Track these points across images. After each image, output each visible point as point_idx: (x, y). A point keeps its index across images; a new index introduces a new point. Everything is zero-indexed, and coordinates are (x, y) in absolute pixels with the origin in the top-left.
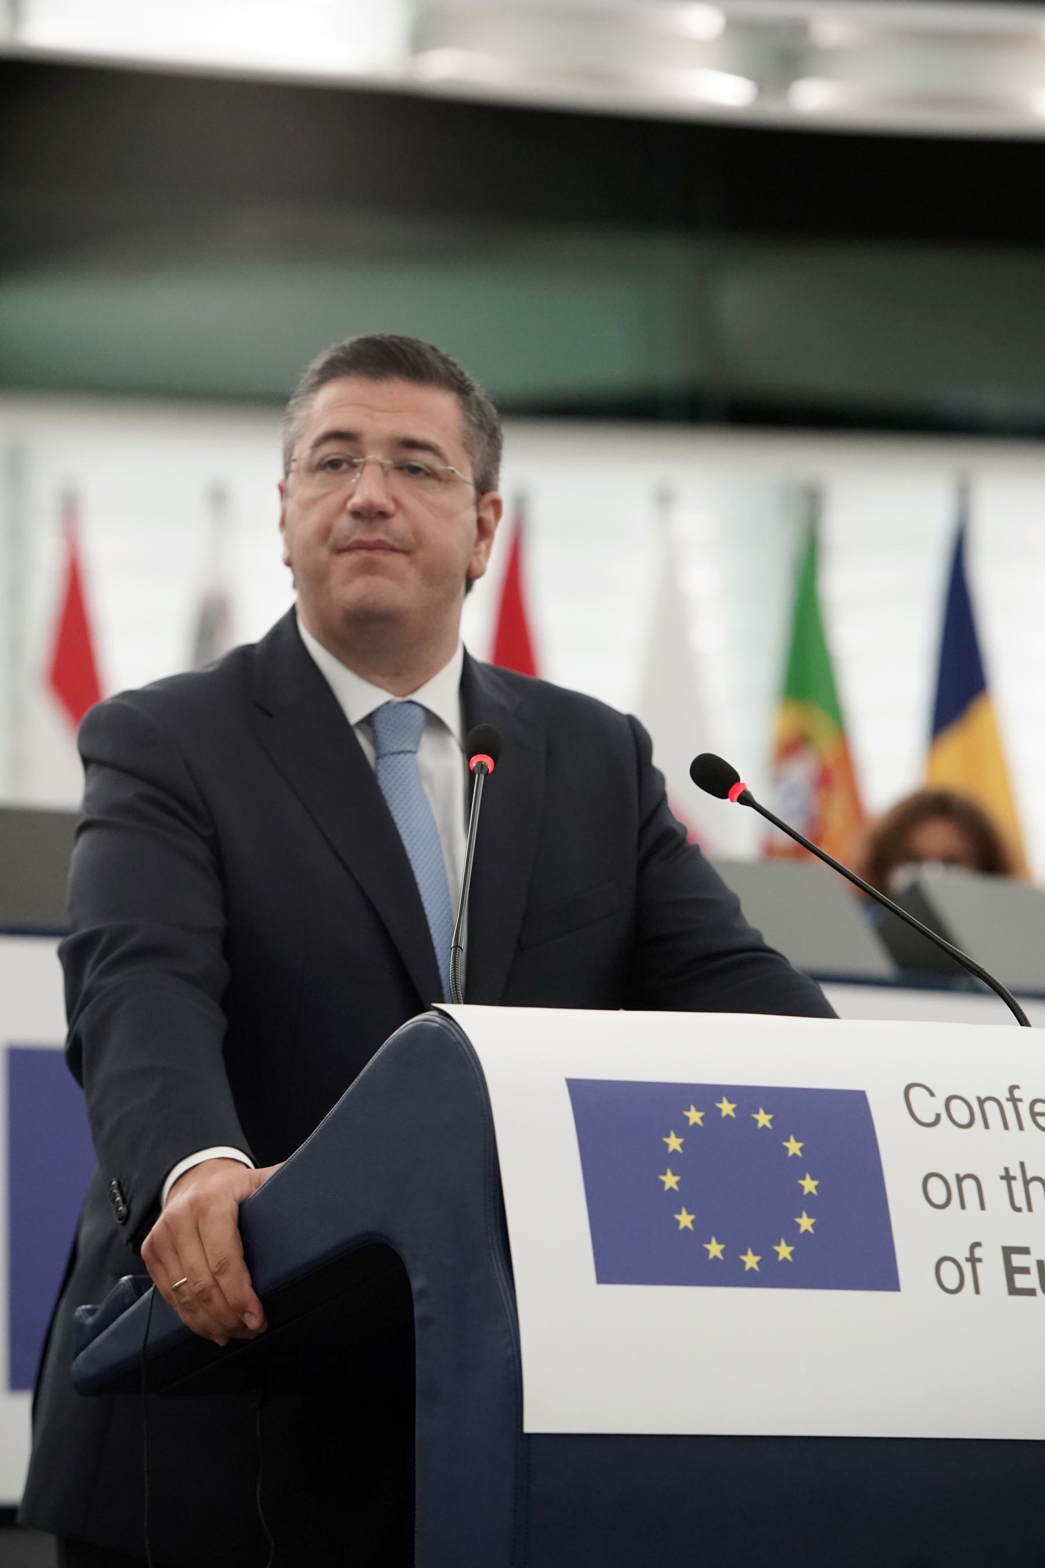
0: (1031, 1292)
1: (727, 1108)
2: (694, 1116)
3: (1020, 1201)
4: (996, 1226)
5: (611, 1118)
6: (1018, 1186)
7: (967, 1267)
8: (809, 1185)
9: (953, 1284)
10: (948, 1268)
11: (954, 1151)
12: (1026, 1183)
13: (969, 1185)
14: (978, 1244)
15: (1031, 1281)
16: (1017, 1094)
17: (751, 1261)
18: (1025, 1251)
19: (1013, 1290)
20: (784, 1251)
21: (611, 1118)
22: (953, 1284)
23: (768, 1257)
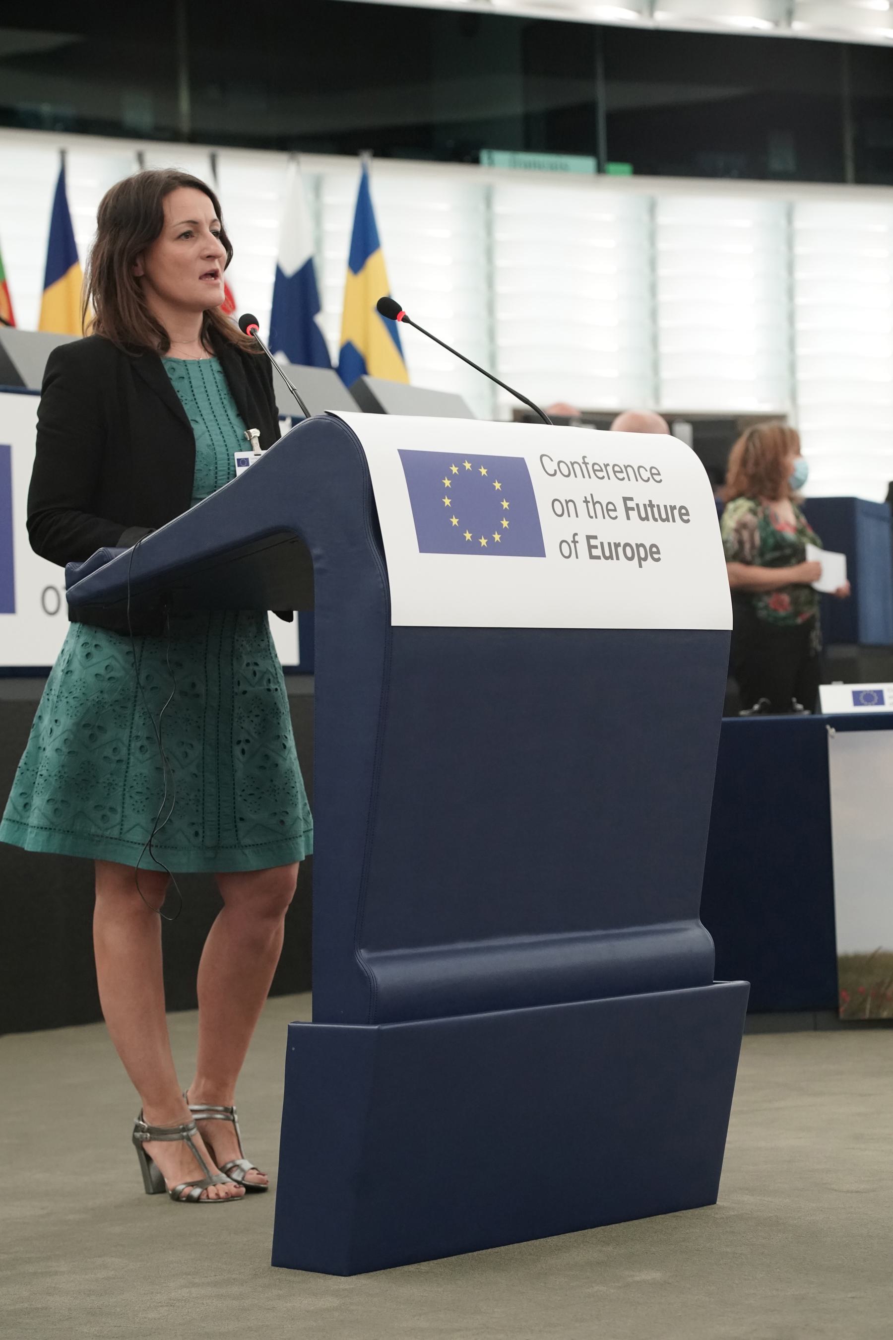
0: (598, 558)
1: (468, 466)
2: (455, 470)
3: (592, 514)
4: (583, 525)
6: (591, 505)
7: (572, 545)
8: (505, 505)
9: (567, 554)
10: (564, 545)
12: (594, 504)
13: (571, 504)
14: (575, 534)
17: (483, 542)
18: (595, 537)
20: (497, 537)
21: (421, 469)
22: (567, 554)
23: (491, 540)
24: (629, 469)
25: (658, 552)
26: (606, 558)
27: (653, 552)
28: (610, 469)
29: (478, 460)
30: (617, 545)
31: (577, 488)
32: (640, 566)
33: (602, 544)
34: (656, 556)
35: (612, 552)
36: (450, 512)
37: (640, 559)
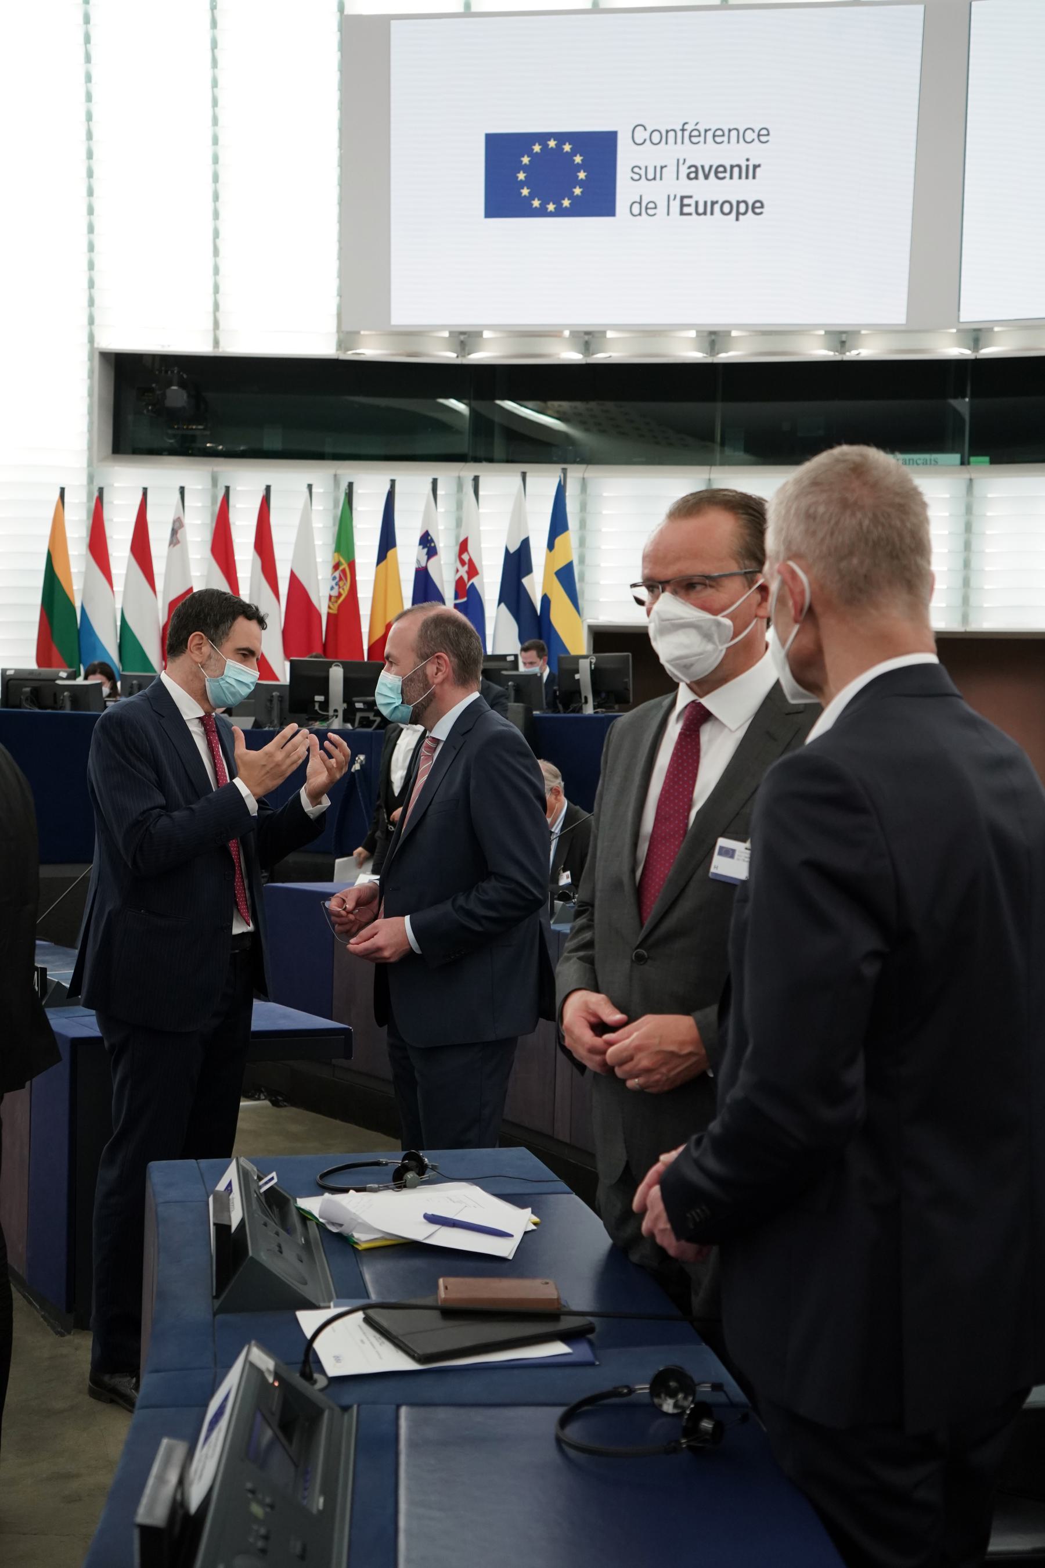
0: (690, 214)
11: (650, 156)
15: (692, 210)
16: (686, 127)
19: (682, 213)
24: (734, 133)
25: (762, 207)
26: (698, 214)
27: (756, 207)
28: (710, 134)
30: (713, 203)
31: (668, 154)
32: (737, 219)
33: (697, 203)
34: (758, 211)
35: (708, 208)
37: (738, 213)
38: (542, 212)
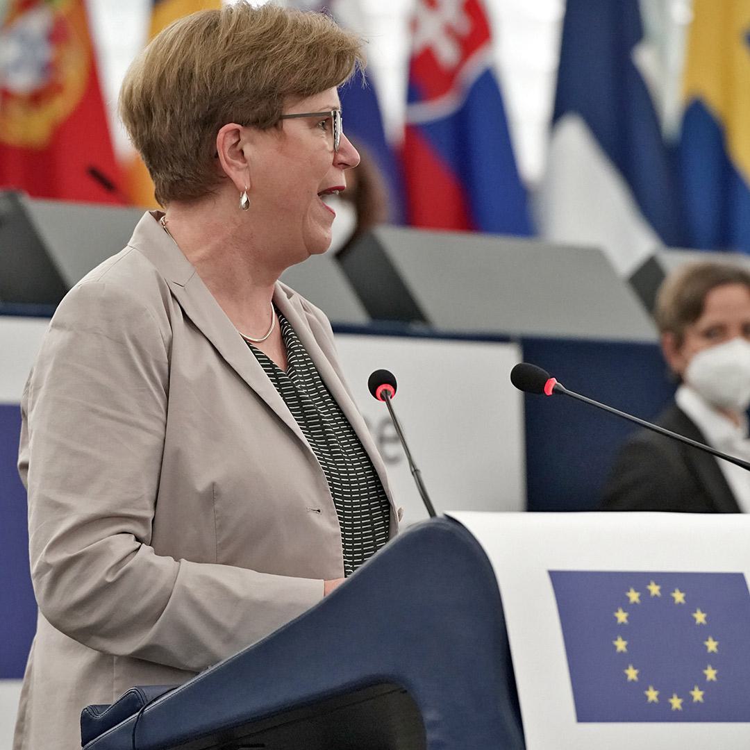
1: (654, 589)
2: (634, 596)
5: (578, 594)
8: (712, 645)
17: (676, 703)
20: (697, 695)
21: (578, 594)
23: (687, 699)
29: (669, 580)
36: (625, 660)
38: (661, 714)
